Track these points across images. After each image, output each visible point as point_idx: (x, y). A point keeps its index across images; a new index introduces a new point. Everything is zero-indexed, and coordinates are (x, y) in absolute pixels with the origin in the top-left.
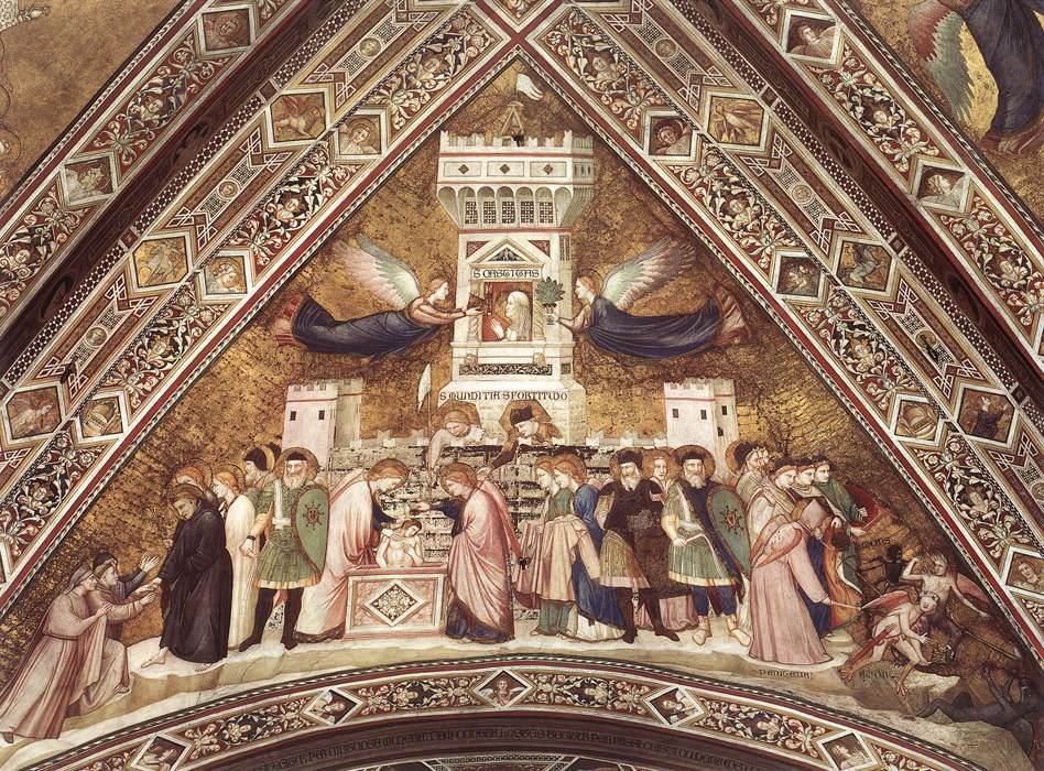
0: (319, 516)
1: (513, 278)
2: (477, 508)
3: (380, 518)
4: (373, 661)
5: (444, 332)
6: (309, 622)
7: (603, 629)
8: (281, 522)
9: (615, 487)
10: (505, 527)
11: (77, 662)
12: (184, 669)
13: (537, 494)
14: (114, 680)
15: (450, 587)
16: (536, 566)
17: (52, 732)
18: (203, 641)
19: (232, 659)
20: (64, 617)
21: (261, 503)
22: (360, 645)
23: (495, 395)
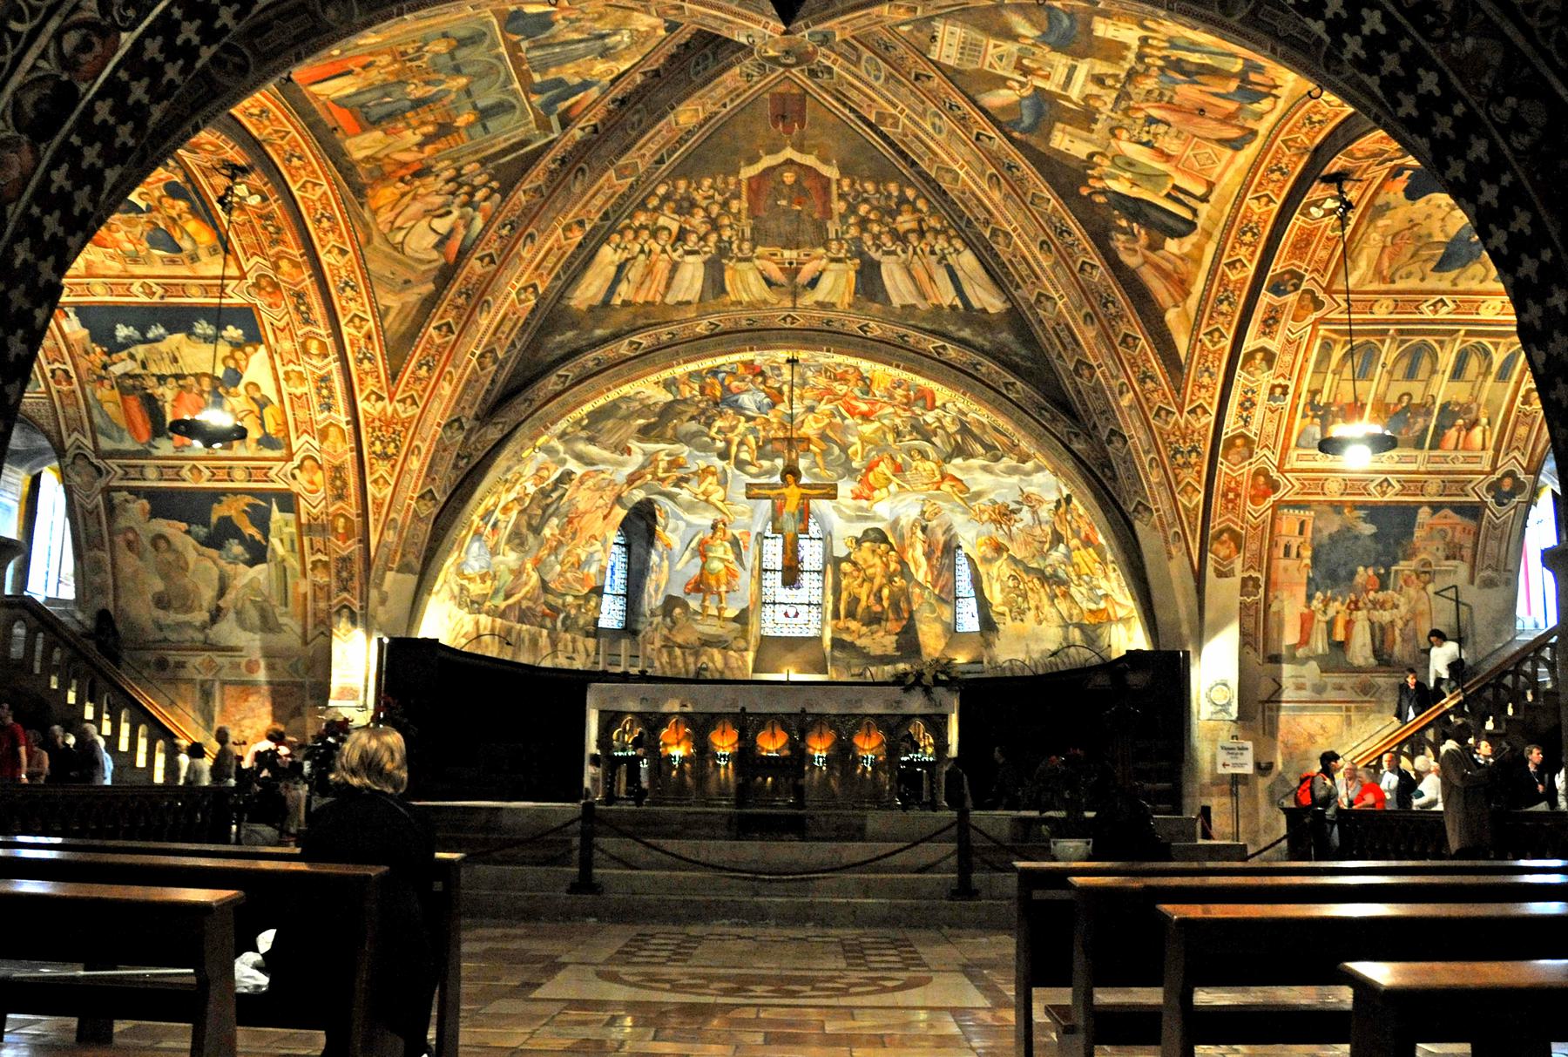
0: (1131, 164)
1: (1014, 59)
2: (1156, 113)
3: (1147, 144)
4: (1239, 179)
5: (1036, 89)
6: (1199, 190)
7: (1265, 104)
8: (1128, 175)
9: (1161, 69)
10: (1171, 106)
11: (1157, 267)
12: (1193, 238)
13: (1156, 93)
14: (1179, 262)
15: (1207, 139)
16: (1207, 108)
17: (1188, 294)
18: (1182, 227)
19: (1200, 222)
20: (1130, 260)
21: (1115, 178)
22: (1226, 178)
23: (1084, 86)
